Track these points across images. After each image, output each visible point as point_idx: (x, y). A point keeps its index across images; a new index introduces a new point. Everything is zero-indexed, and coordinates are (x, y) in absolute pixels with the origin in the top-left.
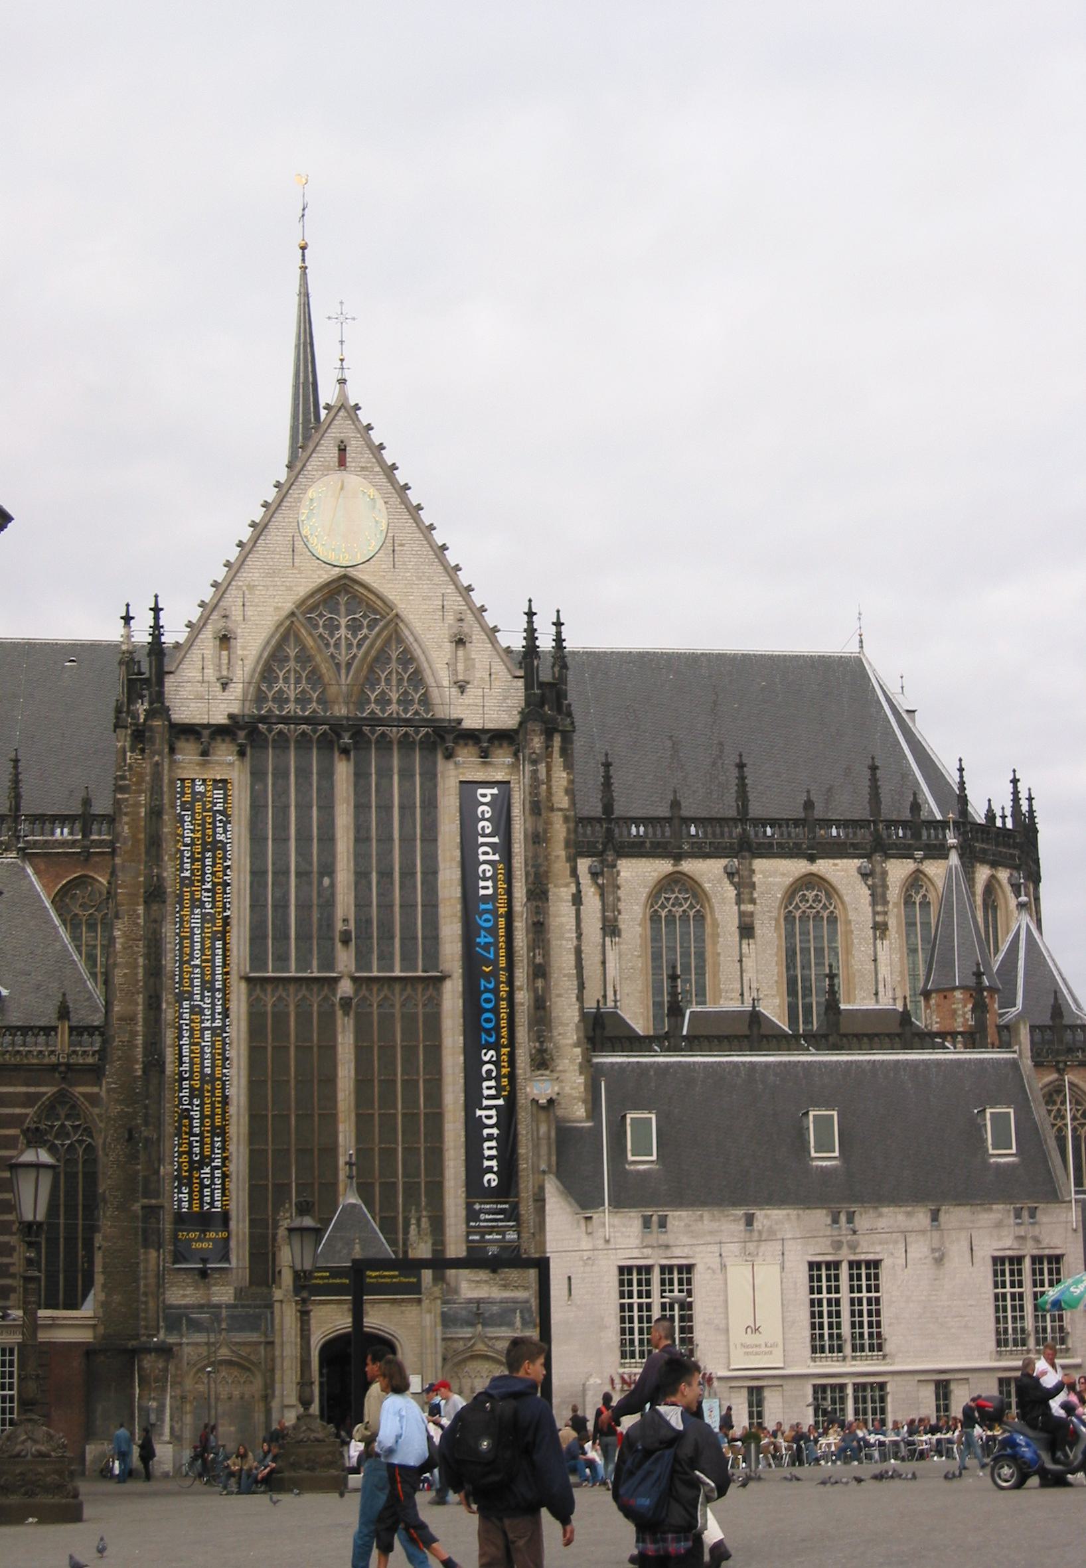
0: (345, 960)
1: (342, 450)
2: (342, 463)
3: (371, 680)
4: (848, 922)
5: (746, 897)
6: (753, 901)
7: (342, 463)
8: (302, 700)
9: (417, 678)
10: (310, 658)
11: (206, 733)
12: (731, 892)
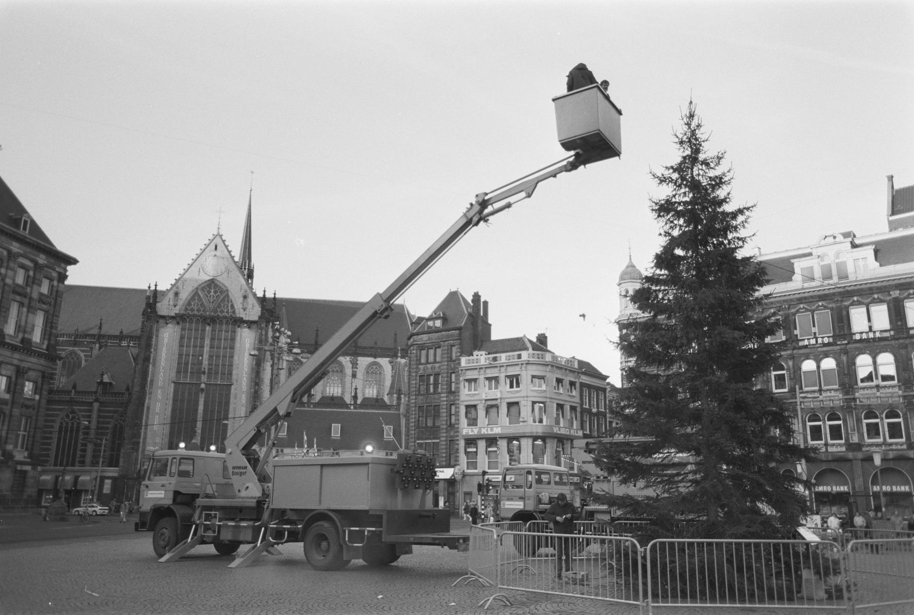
0: (204, 378)
1: (216, 247)
2: (216, 249)
3: (219, 306)
4: (384, 375)
5: (354, 366)
6: (357, 368)
7: (216, 249)
8: (198, 310)
9: (232, 306)
10: (202, 300)
11: (167, 318)
12: (351, 365)
